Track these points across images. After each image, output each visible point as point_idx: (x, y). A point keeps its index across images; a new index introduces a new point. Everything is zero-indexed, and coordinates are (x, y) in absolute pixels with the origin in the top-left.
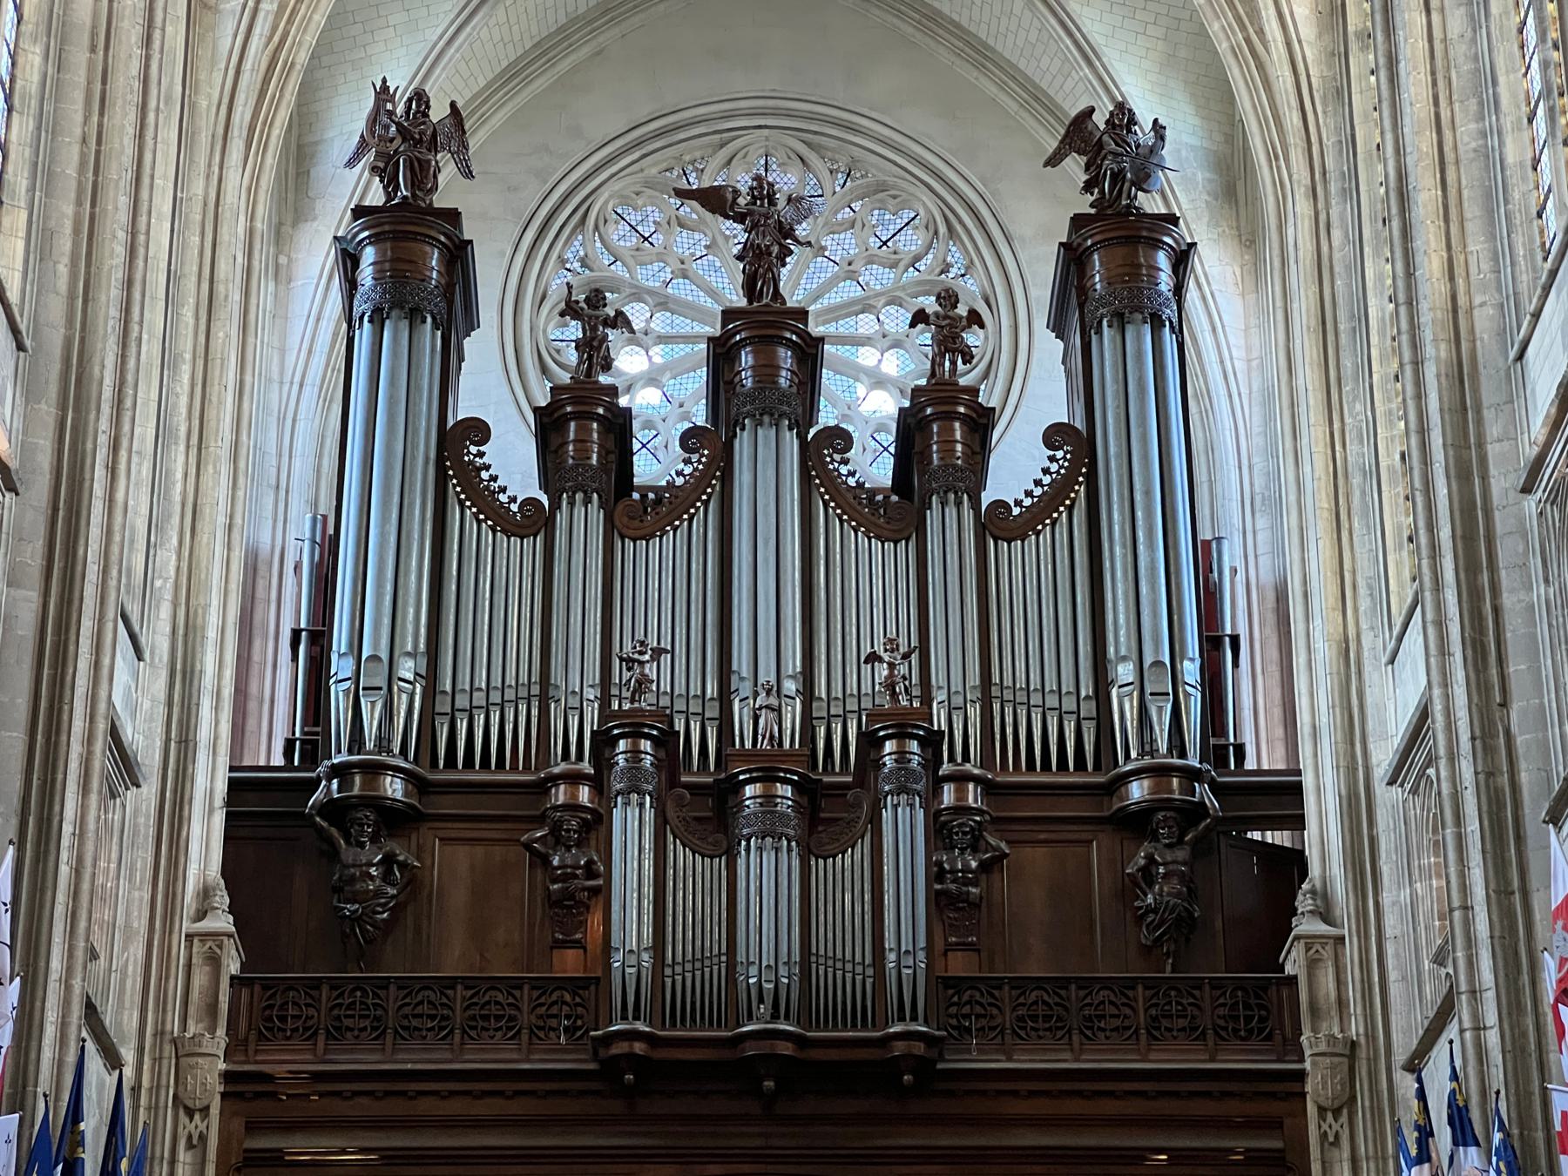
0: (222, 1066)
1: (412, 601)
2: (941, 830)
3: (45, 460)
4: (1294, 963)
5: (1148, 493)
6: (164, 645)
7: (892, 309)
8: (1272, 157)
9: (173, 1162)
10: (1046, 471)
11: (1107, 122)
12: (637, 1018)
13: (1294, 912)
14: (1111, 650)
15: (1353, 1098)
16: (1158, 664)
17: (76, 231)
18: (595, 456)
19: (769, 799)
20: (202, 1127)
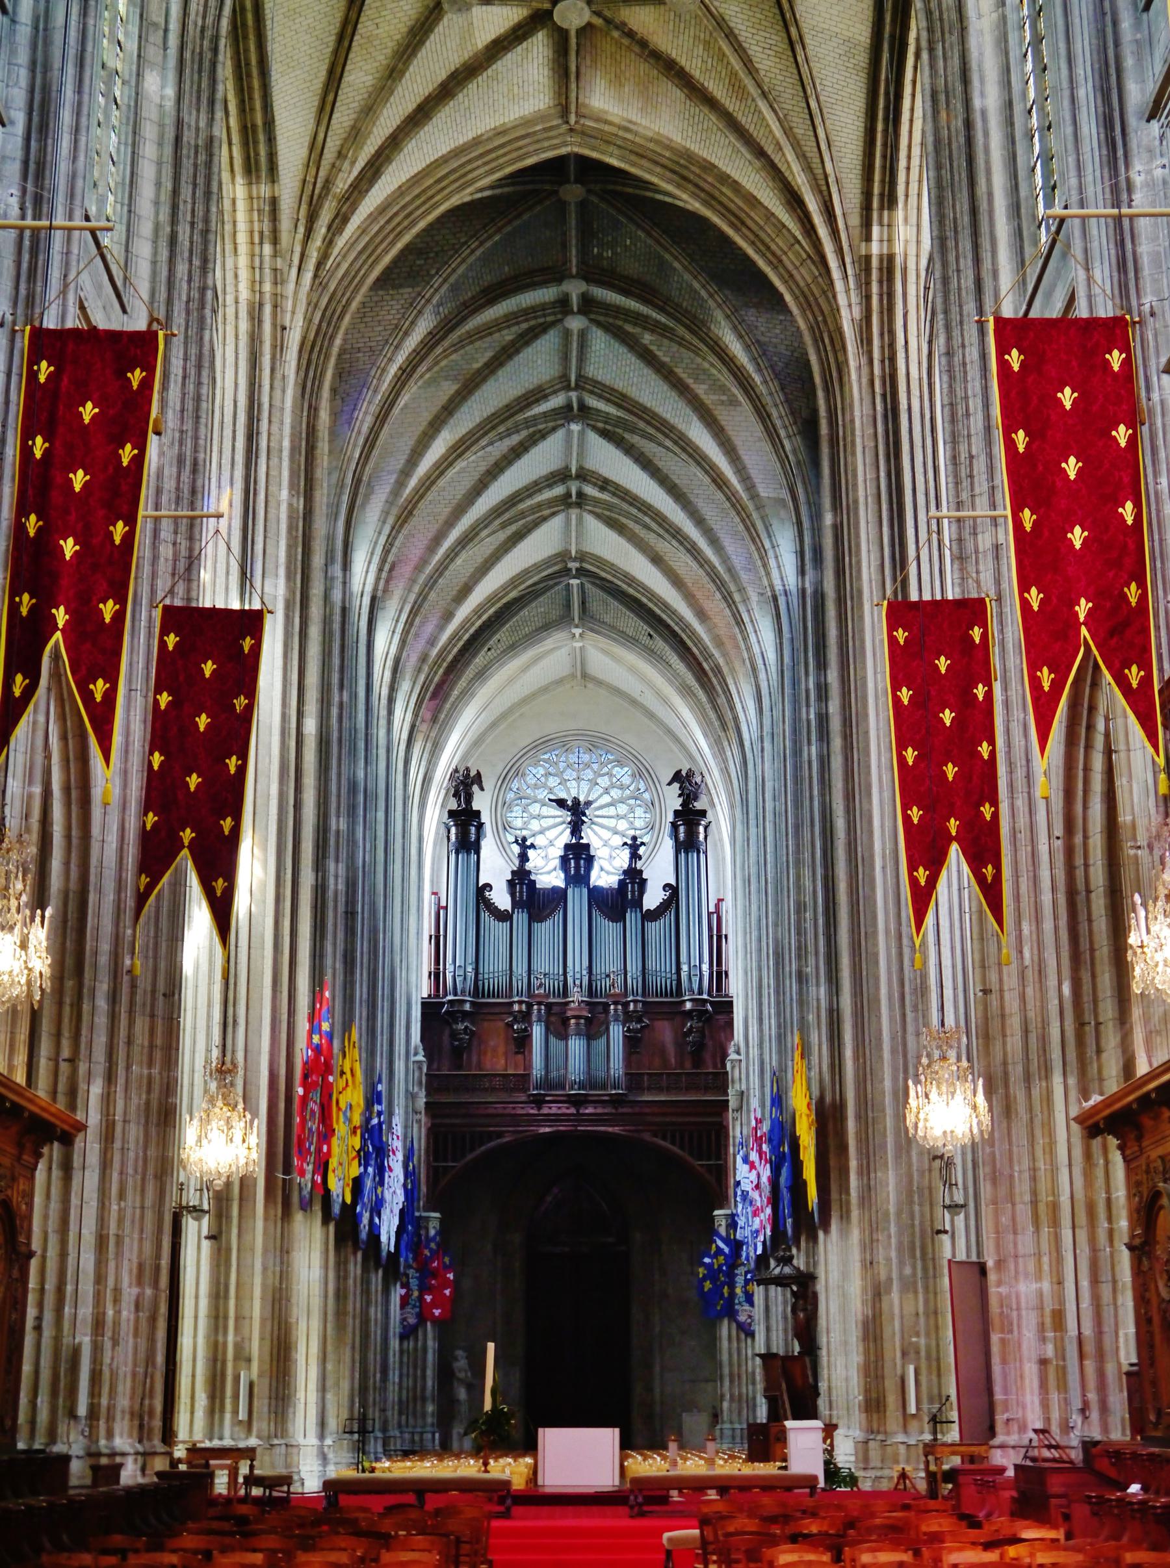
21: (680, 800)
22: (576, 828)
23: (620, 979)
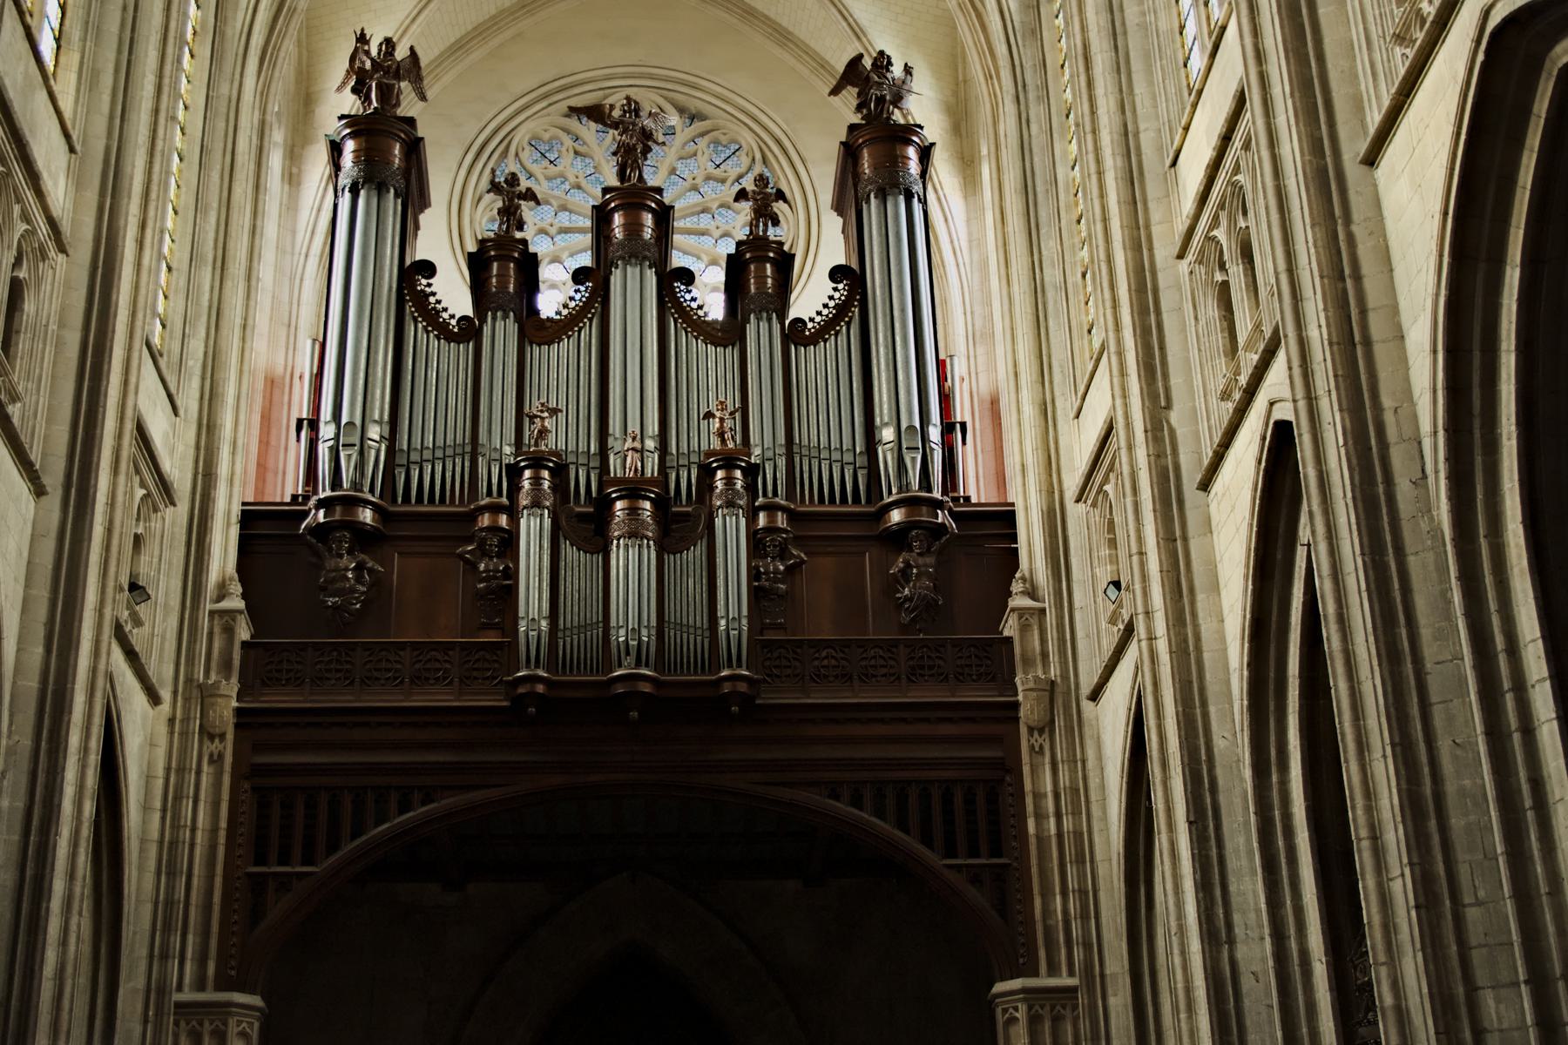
0: (235, 704)
2: (757, 543)
3: (88, 232)
4: (1010, 628)
5: (903, 310)
6: (194, 407)
8: (988, 77)
9: (199, 772)
10: (831, 298)
12: (537, 666)
13: (1010, 594)
14: (878, 420)
16: (911, 427)
17: (117, 71)
19: (633, 511)
20: (220, 747)
22: (631, 156)
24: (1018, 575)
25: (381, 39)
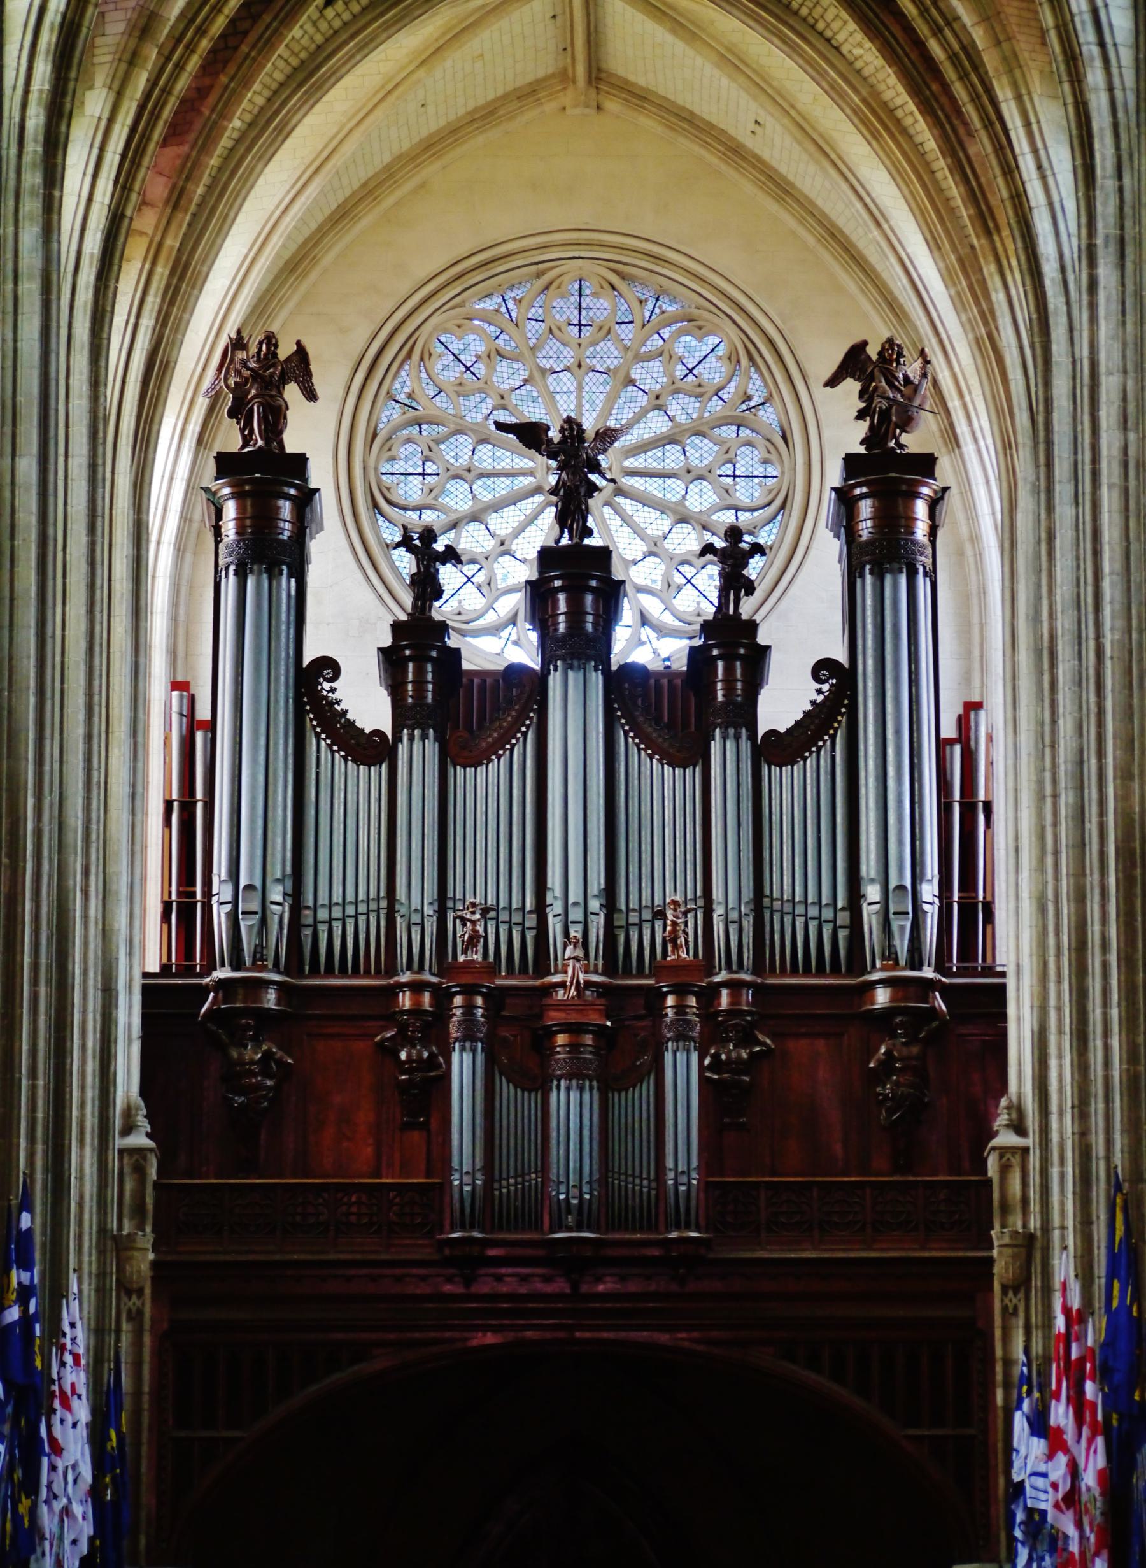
0: (151, 1256)
1: (279, 831)
4: (992, 1165)
5: (898, 732)
7: (696, 440)
9: (118, 1331)
11: (880, 354)
15: (1029, 1279)
16: (901, 888)
18: (430, 695)
20: (138, 1303)
21: (863, 428)
22: (572, 505)
23: (693, 925)
24: (1004, 1102)
25: (261, 337)
